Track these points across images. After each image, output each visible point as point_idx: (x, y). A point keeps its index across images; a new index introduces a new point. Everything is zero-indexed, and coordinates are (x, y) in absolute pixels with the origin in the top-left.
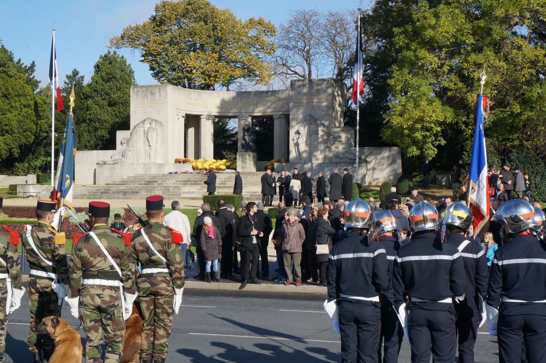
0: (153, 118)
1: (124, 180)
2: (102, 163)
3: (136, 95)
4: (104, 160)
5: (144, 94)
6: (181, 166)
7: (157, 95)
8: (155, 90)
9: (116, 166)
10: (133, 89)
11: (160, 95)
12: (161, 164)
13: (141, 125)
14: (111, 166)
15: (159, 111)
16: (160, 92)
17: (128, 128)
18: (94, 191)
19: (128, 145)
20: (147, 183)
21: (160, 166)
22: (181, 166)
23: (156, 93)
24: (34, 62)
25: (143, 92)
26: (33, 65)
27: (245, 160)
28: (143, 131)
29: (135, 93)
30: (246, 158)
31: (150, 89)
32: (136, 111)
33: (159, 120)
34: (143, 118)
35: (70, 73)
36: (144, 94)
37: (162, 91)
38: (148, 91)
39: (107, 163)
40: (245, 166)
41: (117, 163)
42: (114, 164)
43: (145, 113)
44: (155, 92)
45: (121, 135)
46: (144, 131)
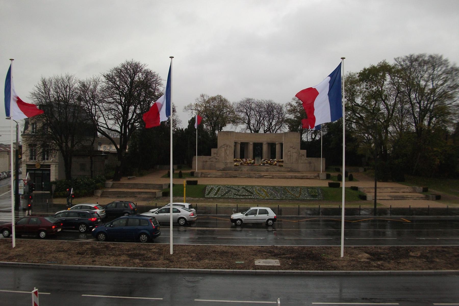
45: (213, 151)
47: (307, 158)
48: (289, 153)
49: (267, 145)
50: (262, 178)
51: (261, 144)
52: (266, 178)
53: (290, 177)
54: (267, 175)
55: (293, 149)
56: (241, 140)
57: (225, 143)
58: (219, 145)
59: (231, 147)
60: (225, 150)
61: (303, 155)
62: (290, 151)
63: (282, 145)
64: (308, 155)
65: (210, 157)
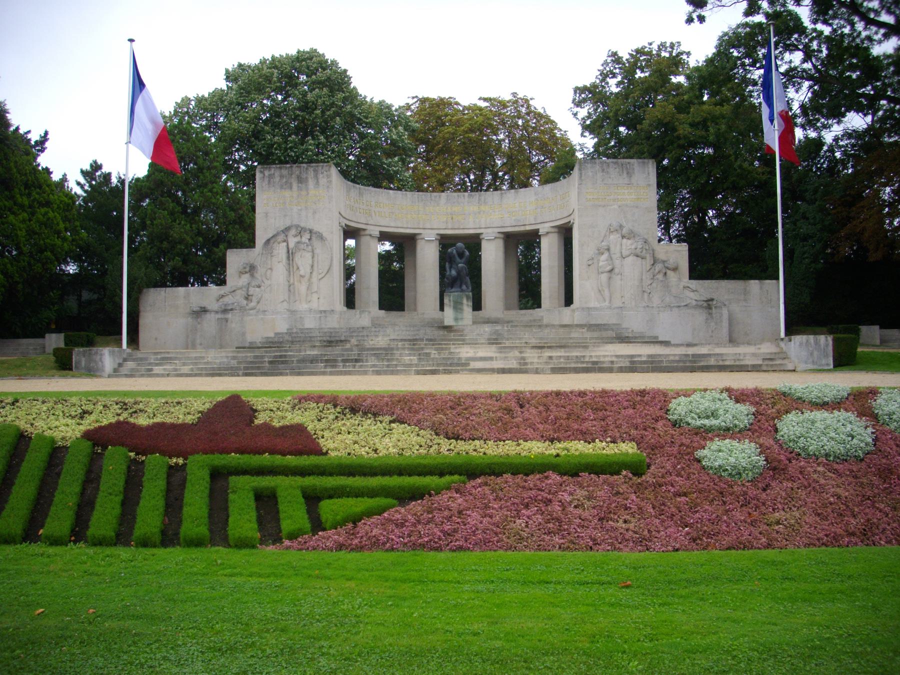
0: (302, 225)
1: (270, 340)
2: (199, 309)
3: (267, 183)
4: (203, 306)
5: (285, 180)
6: (358, 316)
7: (311, 183)
8: (307, 173)
9: (229, 316)
10: (261, 172)
11: (317, 183)
12: (325, 311)
13: (281, 237)
14: (220, 316)
15: (315, 213)
16: (316, 177)
17: (250, 243)
18: (249, 359)
19: (252, 276)
20: (325, 344)
21: (323, 314)
22: (358, 316)
23: (310, 180)
24: (46, 133)
25: (282, 176)
26: (44, 138)
27: (459, 307)
28: (285, 250)
29: (266, 180)
30: (462, 304)
31: (298, 172)
32: (267, 214)
33: (316, 228)
34: (281, 224)
35: (87, 167)
36: (285, 180)
37: (321, 176)
38: (293, 176)
39: (209, 308)
40: (460, 317)
41: (232, 310)
42: (225, 311)
43: (285, 216)
44: (307, 178)
45: (235, 259)
46: (288, 248)
47: (694, 284)
48: (605, 256)
49: (500, 244)
50: (457, 372)
51: (473, 243)
52: (479, 371)
53: (626, 363)
54: (491, 359)
55: (623, 237)
56: (383, 222)
57: (288, 224)
58: (262, 231)
59: (321, 237)
60: (290, 255)
61: (675, 269)
62: (608, 250)
63: (566, 233)
64: (698, 271)
65: (222, 292)
